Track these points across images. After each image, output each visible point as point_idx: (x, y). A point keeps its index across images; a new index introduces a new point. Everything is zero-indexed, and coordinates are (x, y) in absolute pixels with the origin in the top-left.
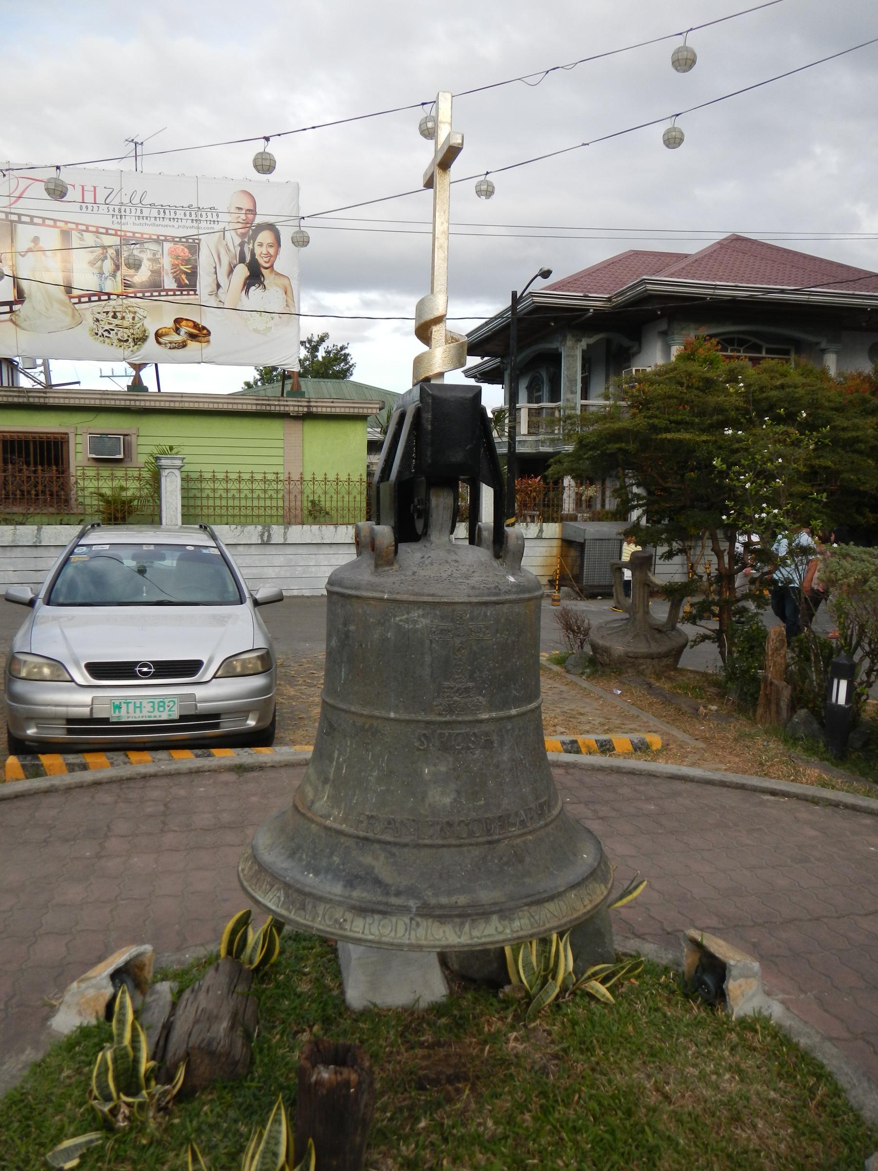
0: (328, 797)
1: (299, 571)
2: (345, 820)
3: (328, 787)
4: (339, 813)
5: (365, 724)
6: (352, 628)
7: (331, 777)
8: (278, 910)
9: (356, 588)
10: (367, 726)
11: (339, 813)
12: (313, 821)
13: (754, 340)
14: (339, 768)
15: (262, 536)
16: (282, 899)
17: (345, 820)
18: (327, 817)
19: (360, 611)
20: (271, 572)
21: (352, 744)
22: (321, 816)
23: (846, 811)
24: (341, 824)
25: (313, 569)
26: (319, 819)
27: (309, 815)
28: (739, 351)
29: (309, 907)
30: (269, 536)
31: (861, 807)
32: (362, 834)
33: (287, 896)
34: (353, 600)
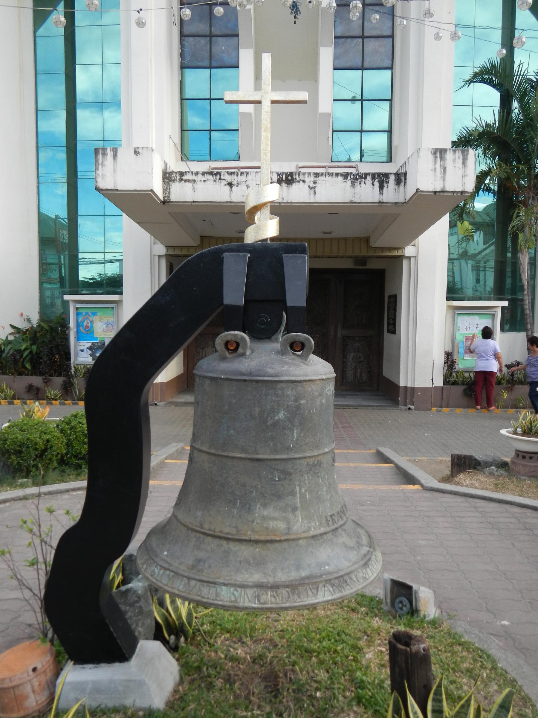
0: (302, 519)
2: (321, 525)
3: (298, 513)
4: (315, 523)
5: (314, 461)
6: (303, 402)
7: (299, 505)
8: (335, 597)
9: (276, 376)
10: (316, 462)
11: (315, 523)
12: (300, 539)
14: (303, 496)
16: (331, 589)
17: (321, 525)
18: (309, 530)
19: (309, 389)
21: (308, 477)
22: (304, 532)
23: (47, 497)
24: (320, 529)
26: (303, 535)
27: (292, 537)
29: (348, 581)
31: (54, 491)
32: (333, 527)
33: (333, 585)
34: (305, 383)
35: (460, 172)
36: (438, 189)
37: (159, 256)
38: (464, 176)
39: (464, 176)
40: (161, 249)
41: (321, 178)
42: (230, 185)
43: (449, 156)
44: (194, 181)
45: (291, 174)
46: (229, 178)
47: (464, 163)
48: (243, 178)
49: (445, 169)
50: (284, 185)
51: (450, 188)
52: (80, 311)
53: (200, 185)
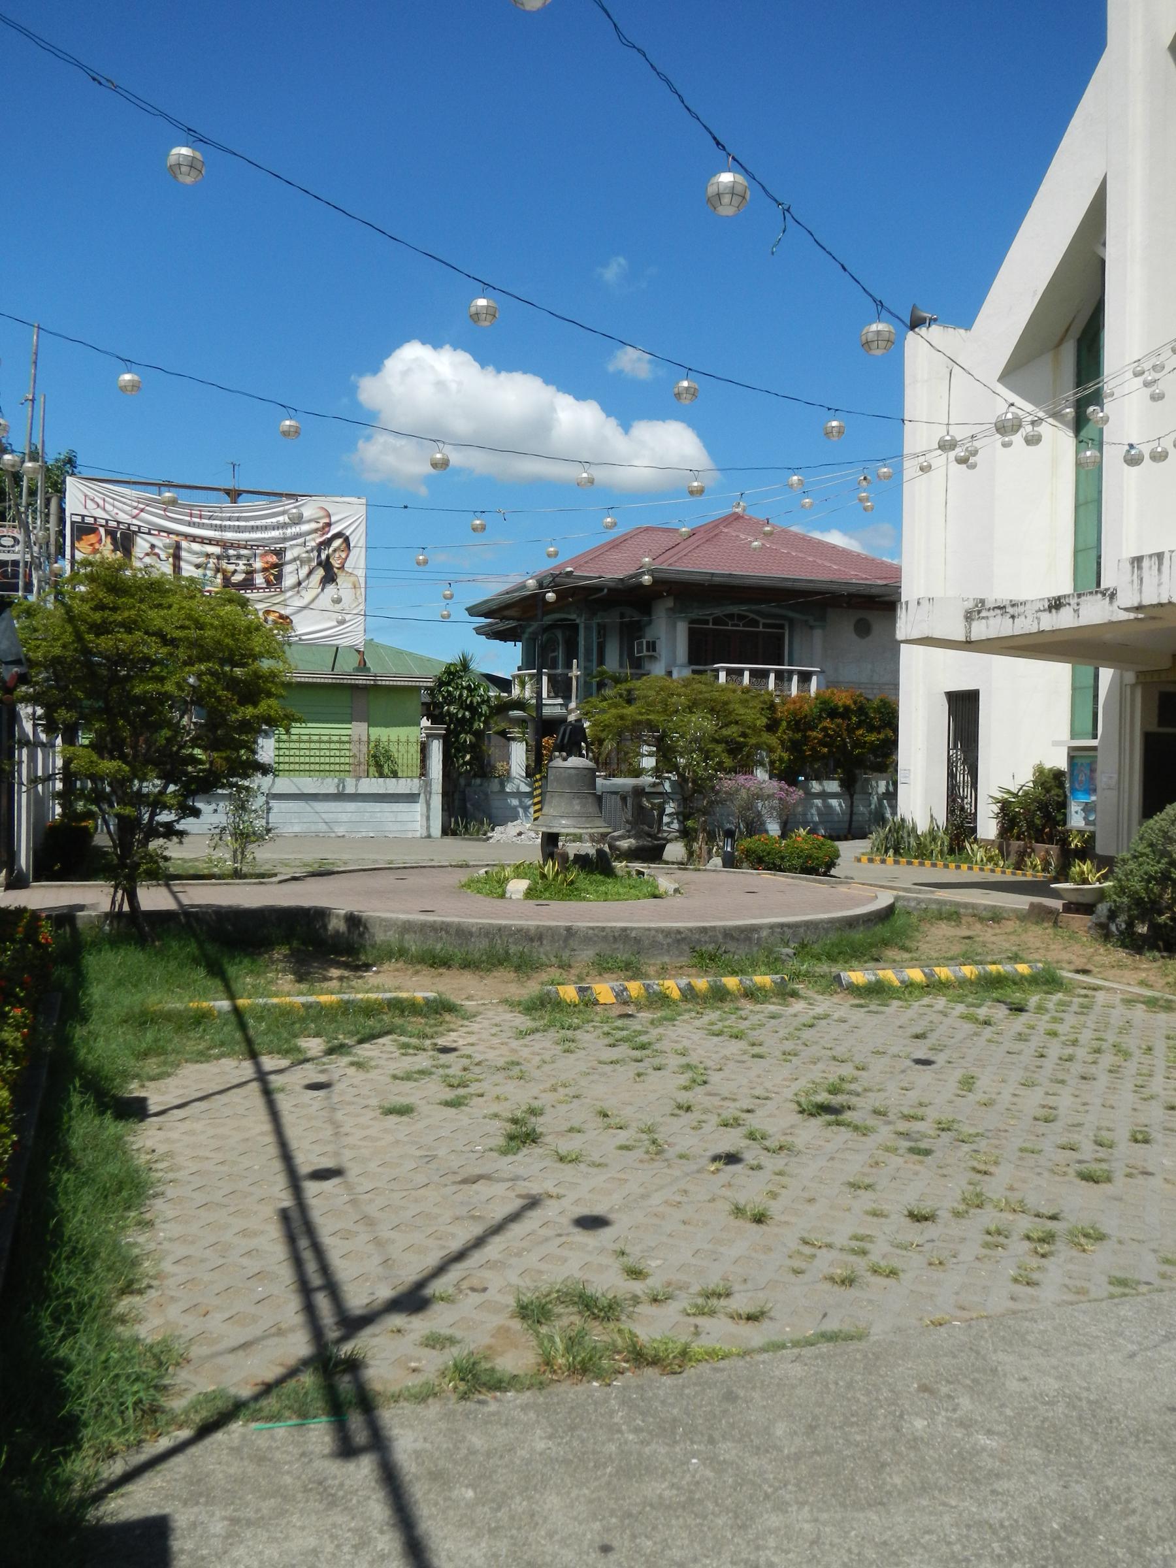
1: (367, 817)
13: (752, 616)
15: (338, 786)
20: (344, 817)
25: (379, 815)
28: (738, 626)
30: (344, 786)
35: (1155, 581)
36: (1136, 605)
37: (1133, 686)
38: (1159, 585)
39: (1159, 585)
40: (1130, 677)
41: (1083, 598)
42: (1013, 617)
43: (1146, 563)
44: (987, 618)
45: (1059, 598)
46: (1010, 610)
47: (1159, 570)
48: (1021, 609)
49: (1141, 580)
50: (1054, 611)
51: (1146, 601)
52: (1076, 761)
53: (992, 621)
